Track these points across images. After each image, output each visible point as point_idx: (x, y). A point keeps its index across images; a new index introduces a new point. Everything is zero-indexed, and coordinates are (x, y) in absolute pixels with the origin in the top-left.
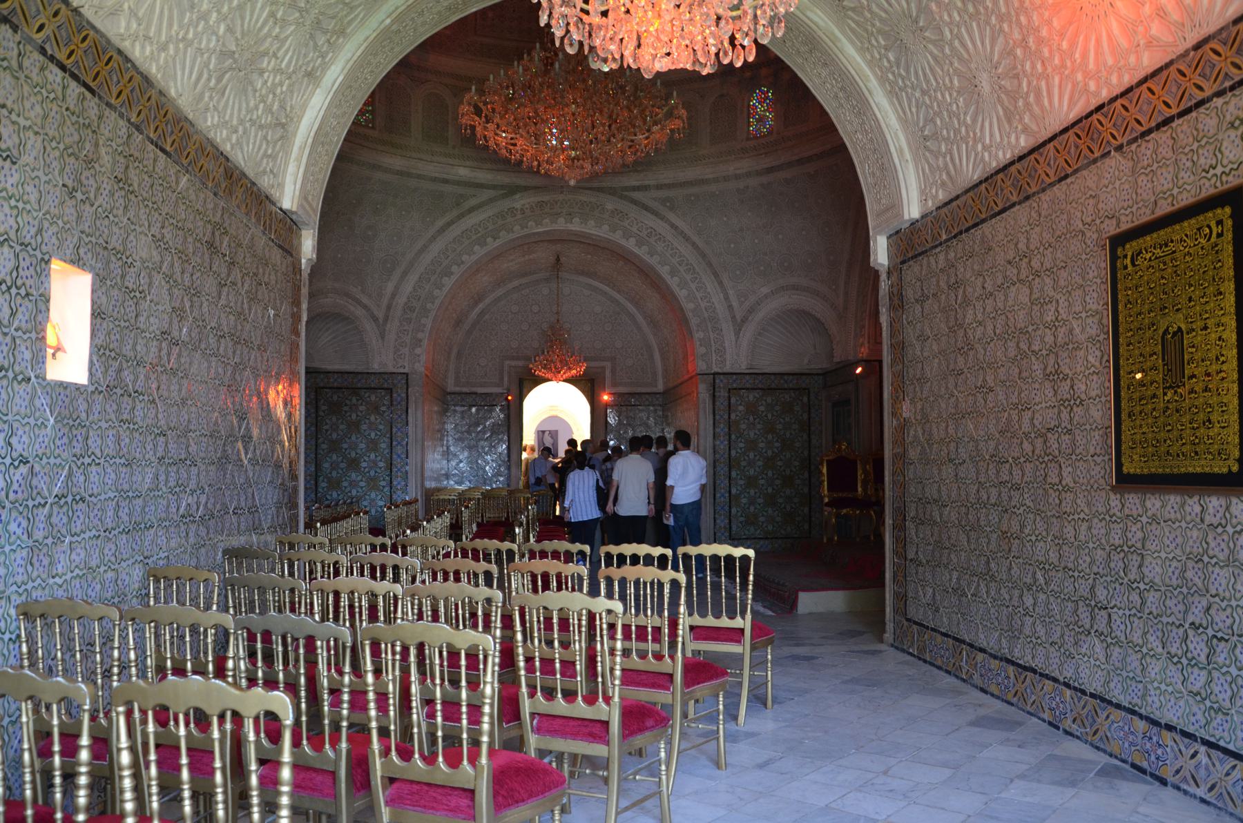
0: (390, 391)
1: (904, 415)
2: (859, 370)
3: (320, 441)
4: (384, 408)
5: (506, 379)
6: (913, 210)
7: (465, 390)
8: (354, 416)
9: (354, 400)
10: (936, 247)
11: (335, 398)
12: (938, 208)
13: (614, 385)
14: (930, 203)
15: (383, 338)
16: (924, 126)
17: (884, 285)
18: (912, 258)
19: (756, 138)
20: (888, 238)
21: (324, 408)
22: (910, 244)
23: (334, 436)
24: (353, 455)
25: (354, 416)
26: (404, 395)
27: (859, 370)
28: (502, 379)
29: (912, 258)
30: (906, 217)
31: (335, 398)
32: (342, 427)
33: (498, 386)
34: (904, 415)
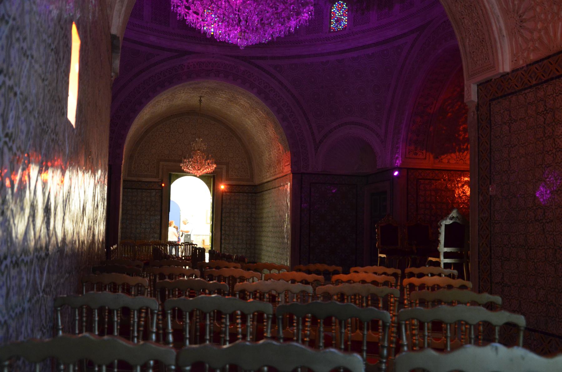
1: (490, 193)
2: (396, 173)
5: (160, 173)
6: (506, 65)
10: (525, 89)
12: (527, 66)
13: (228, 179)
14: (521, 62)
16: (524, 13)
17: (472, 116)
18: (501, 97)
19: (334, 31)
20: (478, 86)
22: (497, 89)
27: (396, 173)
29: (501, 97)
30: (501, 71)
34: (490, 193)
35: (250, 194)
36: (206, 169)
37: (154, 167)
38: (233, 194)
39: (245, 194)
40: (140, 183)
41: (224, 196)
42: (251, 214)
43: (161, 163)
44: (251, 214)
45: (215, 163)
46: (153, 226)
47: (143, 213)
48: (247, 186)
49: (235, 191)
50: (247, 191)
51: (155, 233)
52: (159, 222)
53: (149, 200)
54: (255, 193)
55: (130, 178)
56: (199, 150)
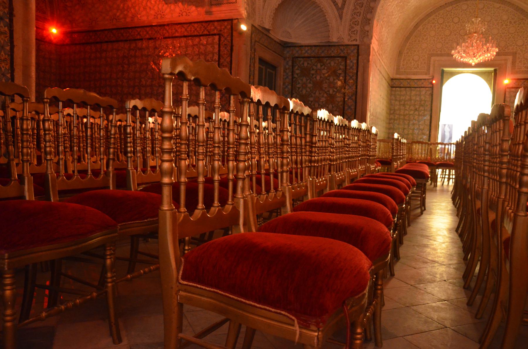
0: (345, 58)
4: (340, 72)
5: (431, 69)
7: (403, 77)
8: (318, 78)
9: (319, 65)
11: (306, 64)
13: (513, 73)
15: (341, 18)
21: (298, 72)
23: (304, 92)
25: (318, 78)
26: (355, 61)
28: (429, 69)
32: (310, 85)
33: (426, 74)
36: (483, 54)
37: (425, 63)
40: (409, 81)
41: (507, 93)
43: (433, 58)
45: (496, 47)
46: (421, 127)
47: (412, 112)
51: (424, 134)
52: (428, 123)
53: (418, 99)
55: (398, 76)
56: (475, 33)
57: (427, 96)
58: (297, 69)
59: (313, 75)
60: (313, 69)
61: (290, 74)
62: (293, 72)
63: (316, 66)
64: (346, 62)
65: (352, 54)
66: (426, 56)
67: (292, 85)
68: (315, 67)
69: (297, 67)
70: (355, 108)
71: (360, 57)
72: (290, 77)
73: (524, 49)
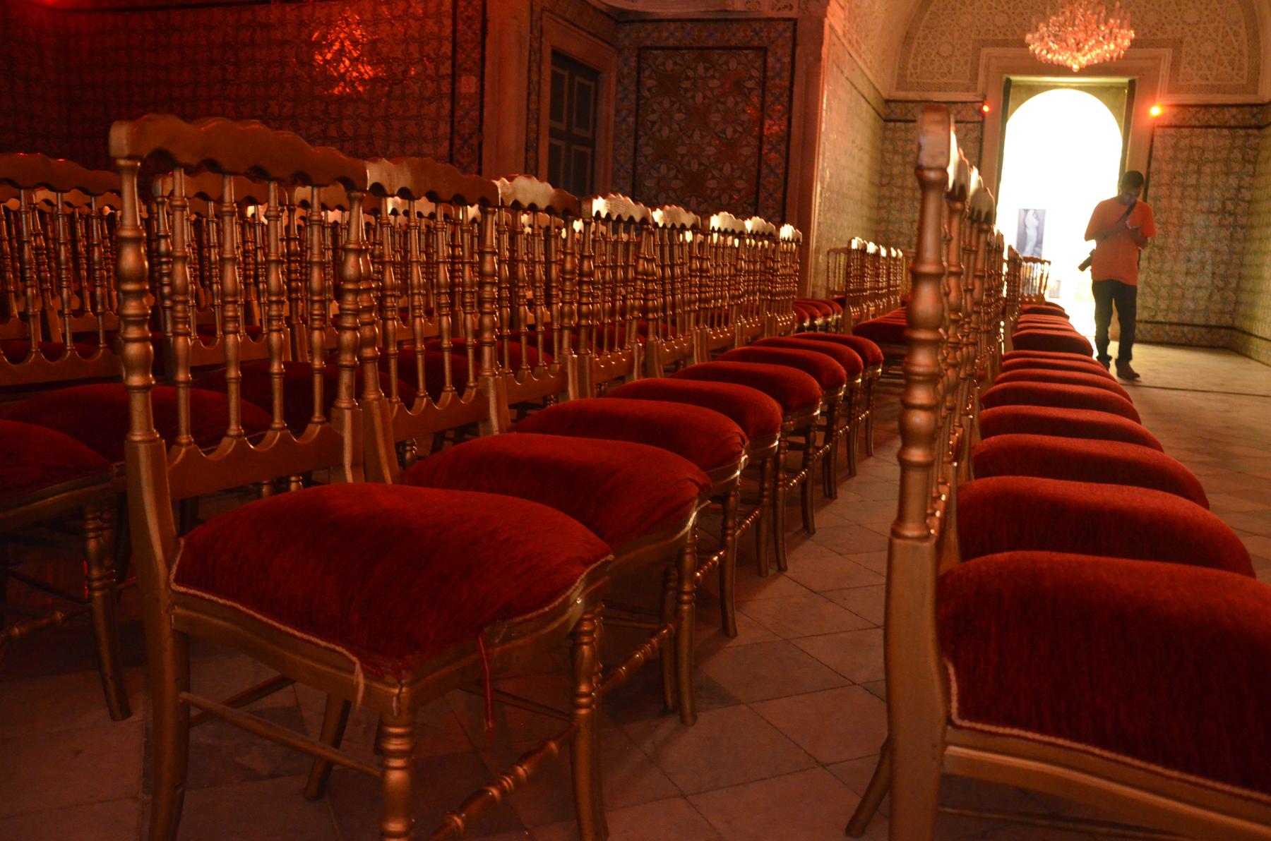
0: (763, 51)
3: (643, 140)
5: (981, 77)
7: (912, 95)
8: (699, 98)
9: (701, 71)
11: (669, 65)
13: (1173, 90)
21: (650, 83)
24: (695, 166)
25: (699, 98)
26: (787, 60)
31: (669, 65)
32: (679, 116)
35: (1242, 132)
38: (1185, 131)
39: (1225, 132)
42: (1239, 189)
43: (985, 51)
44: (1239, 189)
45: (1132, 26)
48: (1232, 106)
49: (1194, 122)
50: (1233, 122)
54: (1259, 128)
55: (901, 95)
57: (970, 144)
58: (650, 77)
59: (686, 90)
60: (687, 78)
61: (632, 88)
62: (639, 83)
63: (695, 70)
64: (765, 62)
65: (780, 42)
66: (970, 47)
67: (637, 117)
68: (690, 73)
69: (647, 73)
70: (786, 174)
71: (798, 49)
72: (633, 97)
73: (1200, 33)
